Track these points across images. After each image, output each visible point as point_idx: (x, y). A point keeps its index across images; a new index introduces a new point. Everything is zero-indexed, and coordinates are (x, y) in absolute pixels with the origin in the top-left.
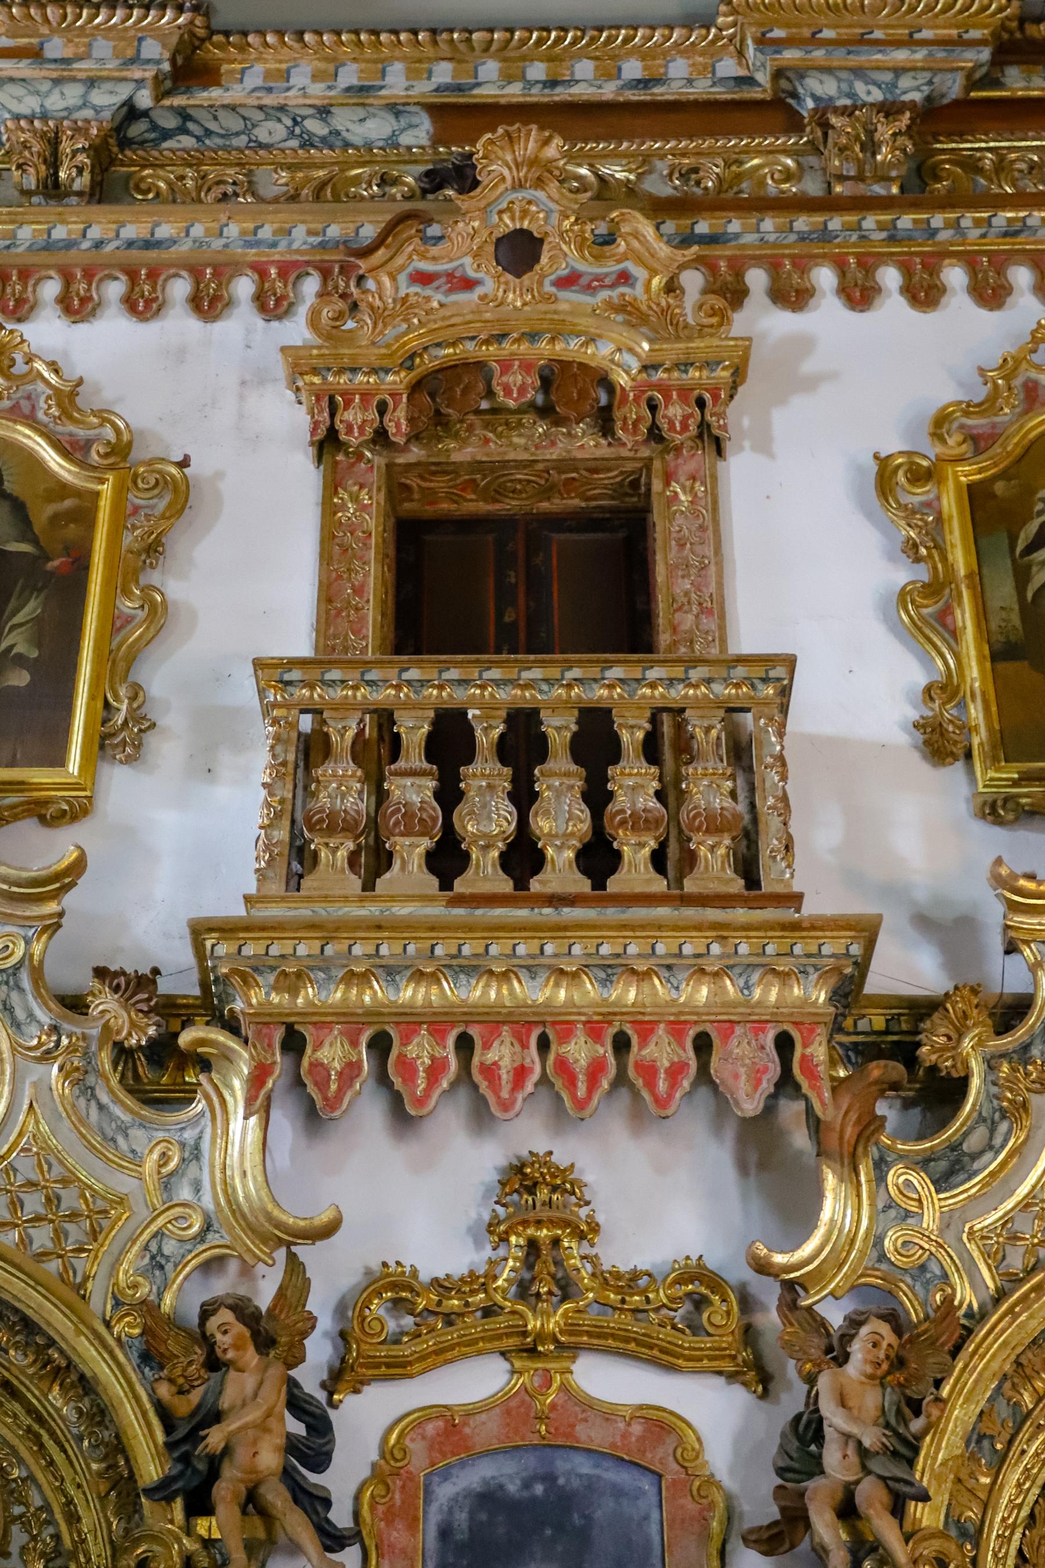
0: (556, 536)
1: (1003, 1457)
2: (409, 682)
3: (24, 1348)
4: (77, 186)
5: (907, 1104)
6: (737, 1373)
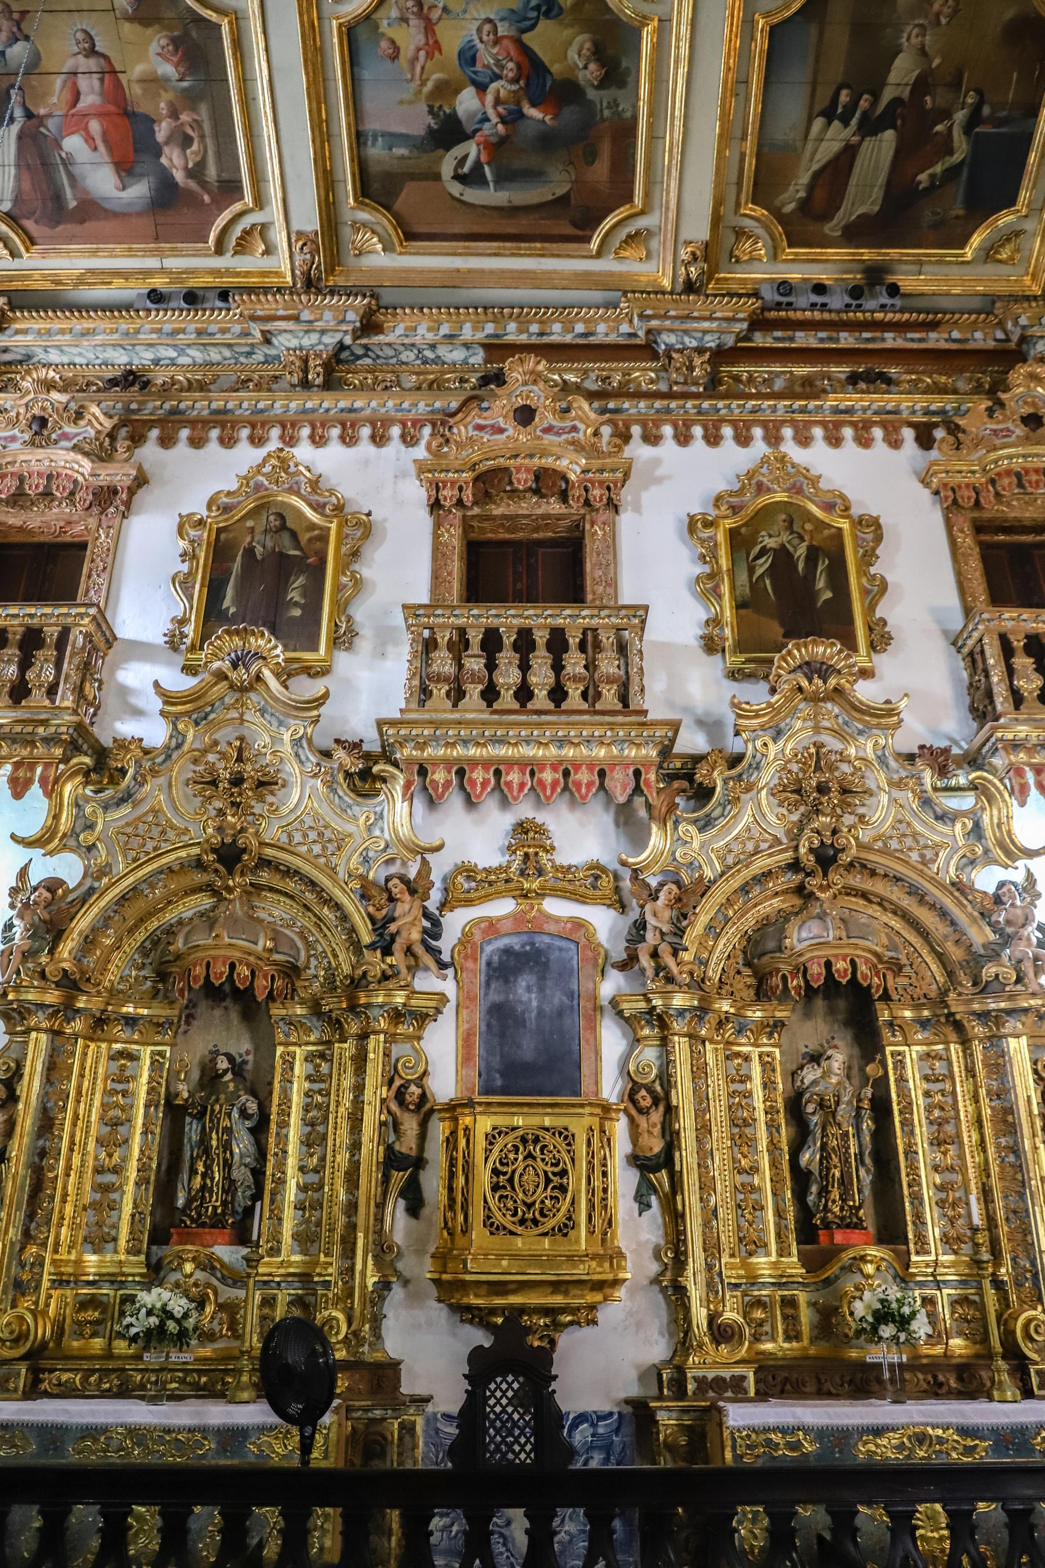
3: (312, 892)
4: (317, 382)
5: (689, 798)
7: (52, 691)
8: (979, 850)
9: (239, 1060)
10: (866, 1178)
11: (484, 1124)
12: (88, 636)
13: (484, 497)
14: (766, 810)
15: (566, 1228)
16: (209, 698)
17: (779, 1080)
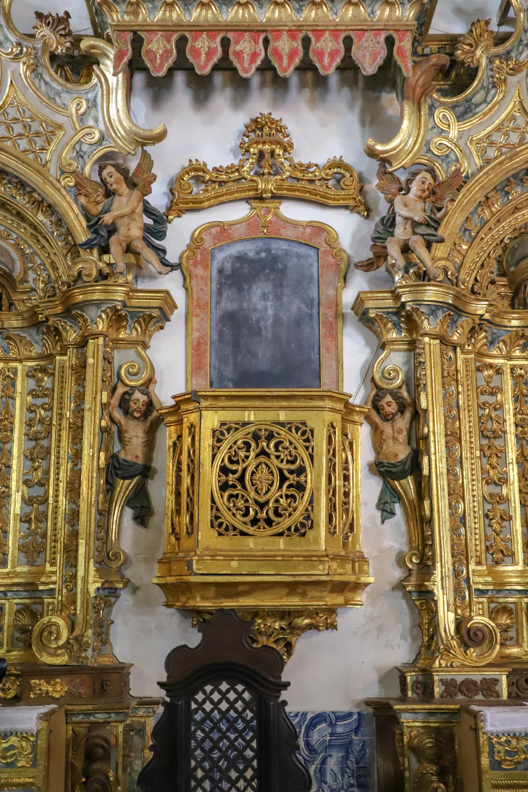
6: (356, 206)
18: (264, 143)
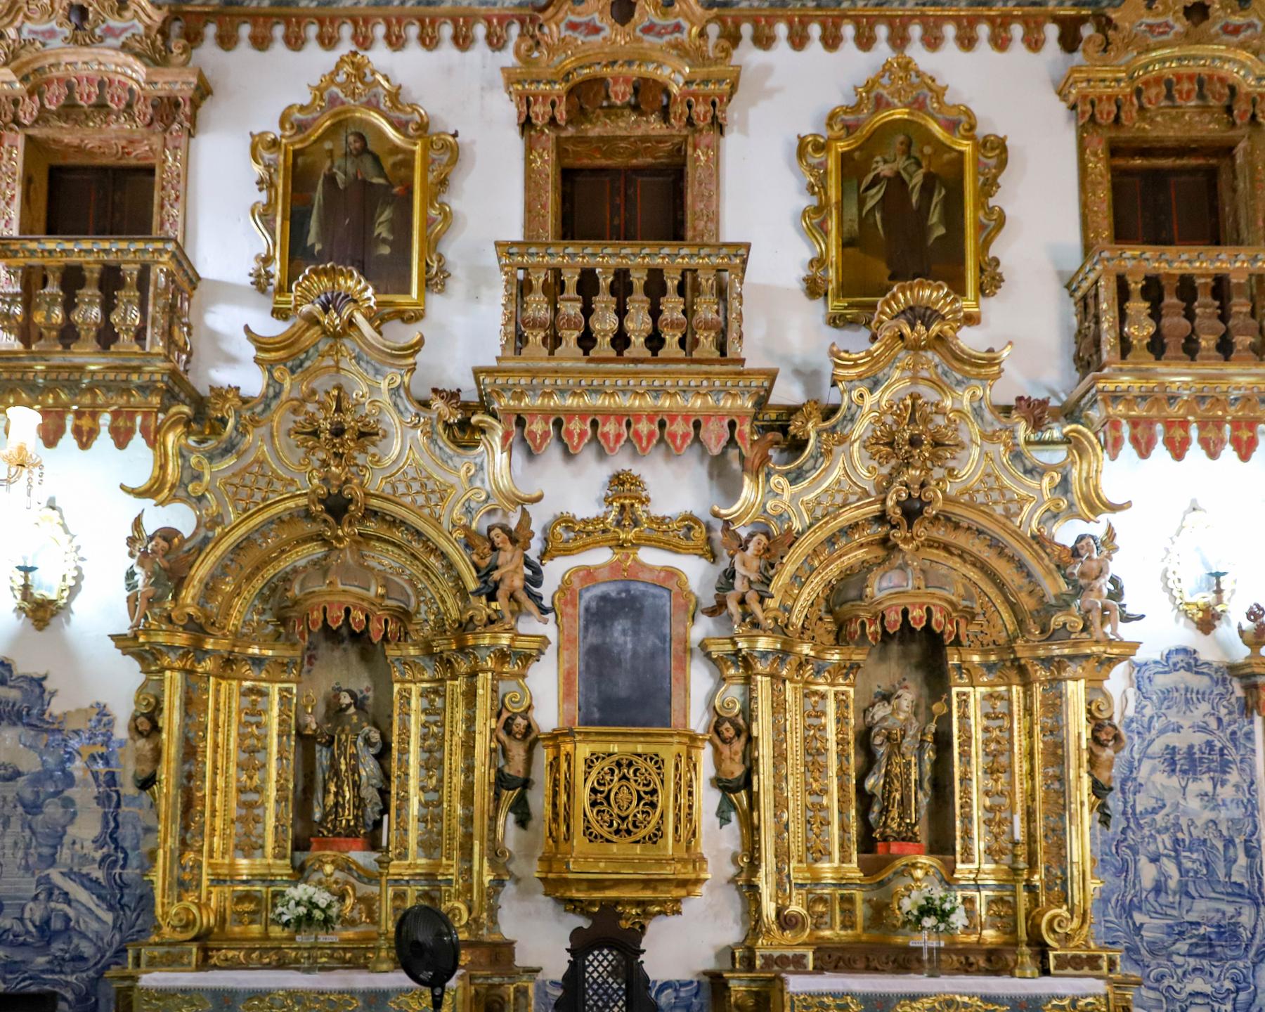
0: (640, 179)
1: (804, 584)
2: (569, 255)
3: (418, 541)
5: (782, 451)
7: (140, 335)
8: (1064, 505)
9: (360, 696)
10: (924, 800)
11: (584, 751)
12: (169, 274)
13: (579, 114)
14: (857, 463)
15: (655, 837)
16: (302, 345)
17: (851, 715)
18: (625, 498)
